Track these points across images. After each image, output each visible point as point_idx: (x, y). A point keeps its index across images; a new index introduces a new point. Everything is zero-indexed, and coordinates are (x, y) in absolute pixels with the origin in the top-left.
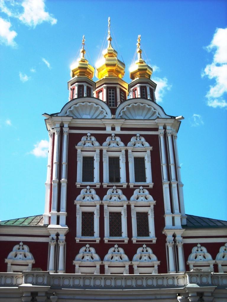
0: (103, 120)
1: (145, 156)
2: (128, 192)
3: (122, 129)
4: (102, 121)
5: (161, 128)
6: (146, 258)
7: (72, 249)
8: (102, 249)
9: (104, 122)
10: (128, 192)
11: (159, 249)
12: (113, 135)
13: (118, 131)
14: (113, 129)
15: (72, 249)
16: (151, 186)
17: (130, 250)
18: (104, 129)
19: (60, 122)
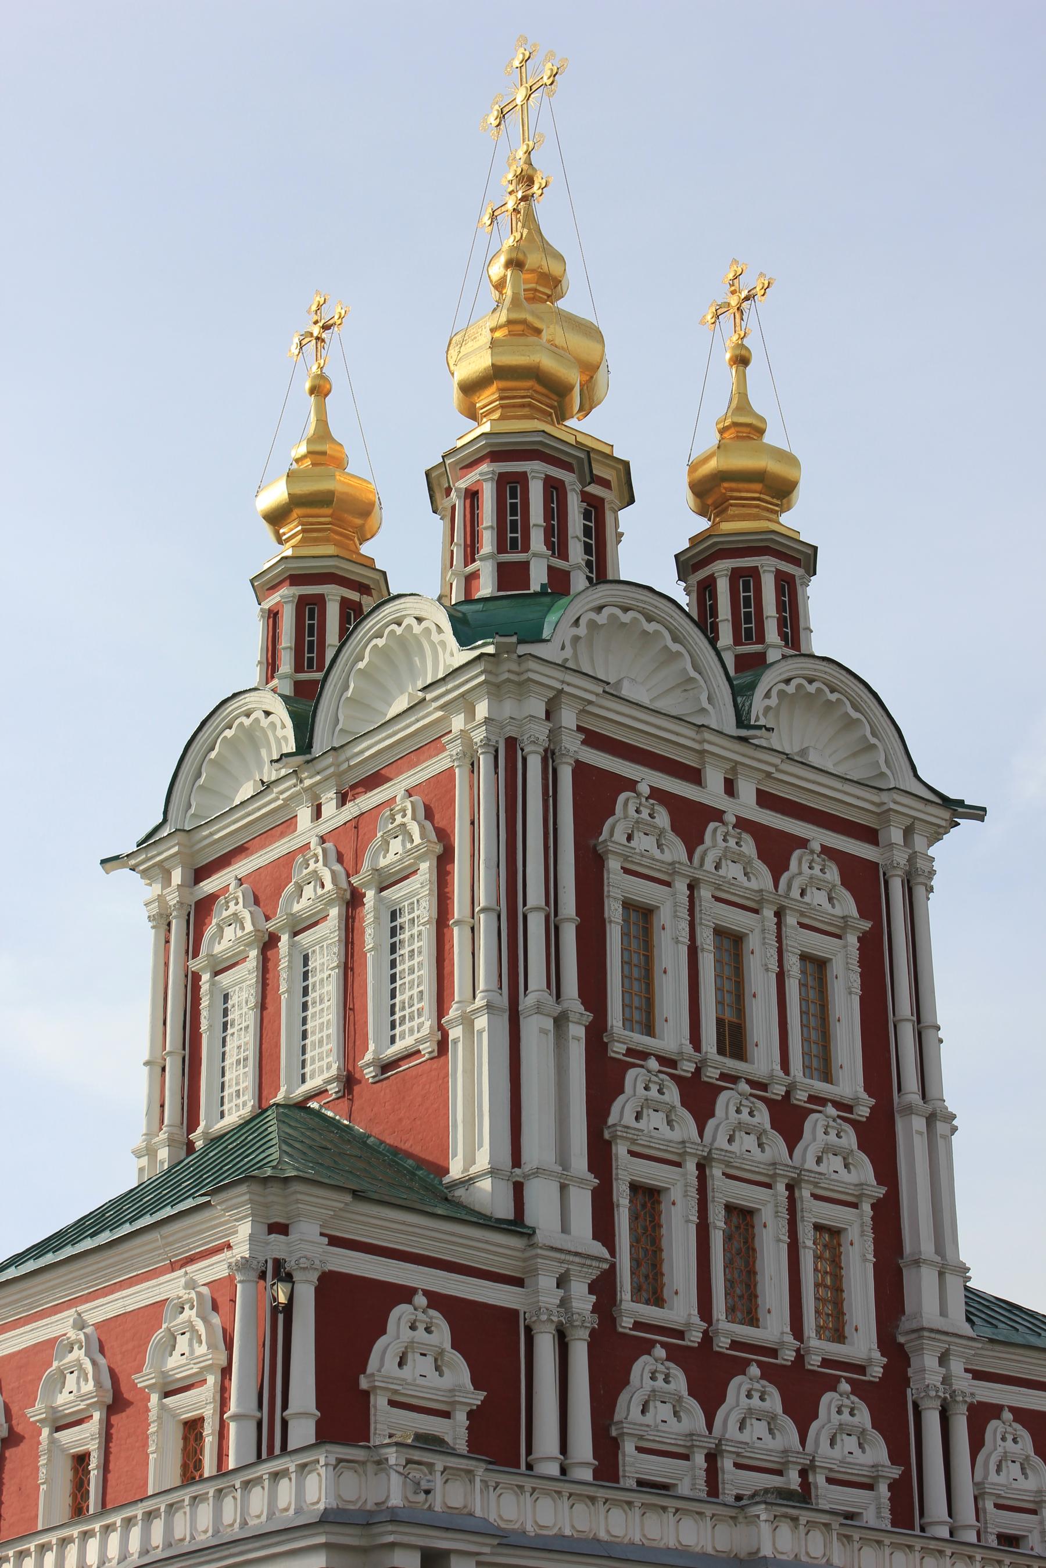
0: (707, 735)
1: (835, 955)
2: (788, 1119)
3: (765, 799)
4: (698, 737)
5: (896, 835)
6: (846, 1437)
7: (613, 1356)
8: (708, 1373)
9: (707, 747)
10: (788, 1119)
11: (890, 1402)
12: (730, 819)
13: (746, 803)
14: (730, 788)
15: (613, 1356)
16: (863, 1112)
17: (801, 1390)
18: (694, 776)
19: (551, 694)
